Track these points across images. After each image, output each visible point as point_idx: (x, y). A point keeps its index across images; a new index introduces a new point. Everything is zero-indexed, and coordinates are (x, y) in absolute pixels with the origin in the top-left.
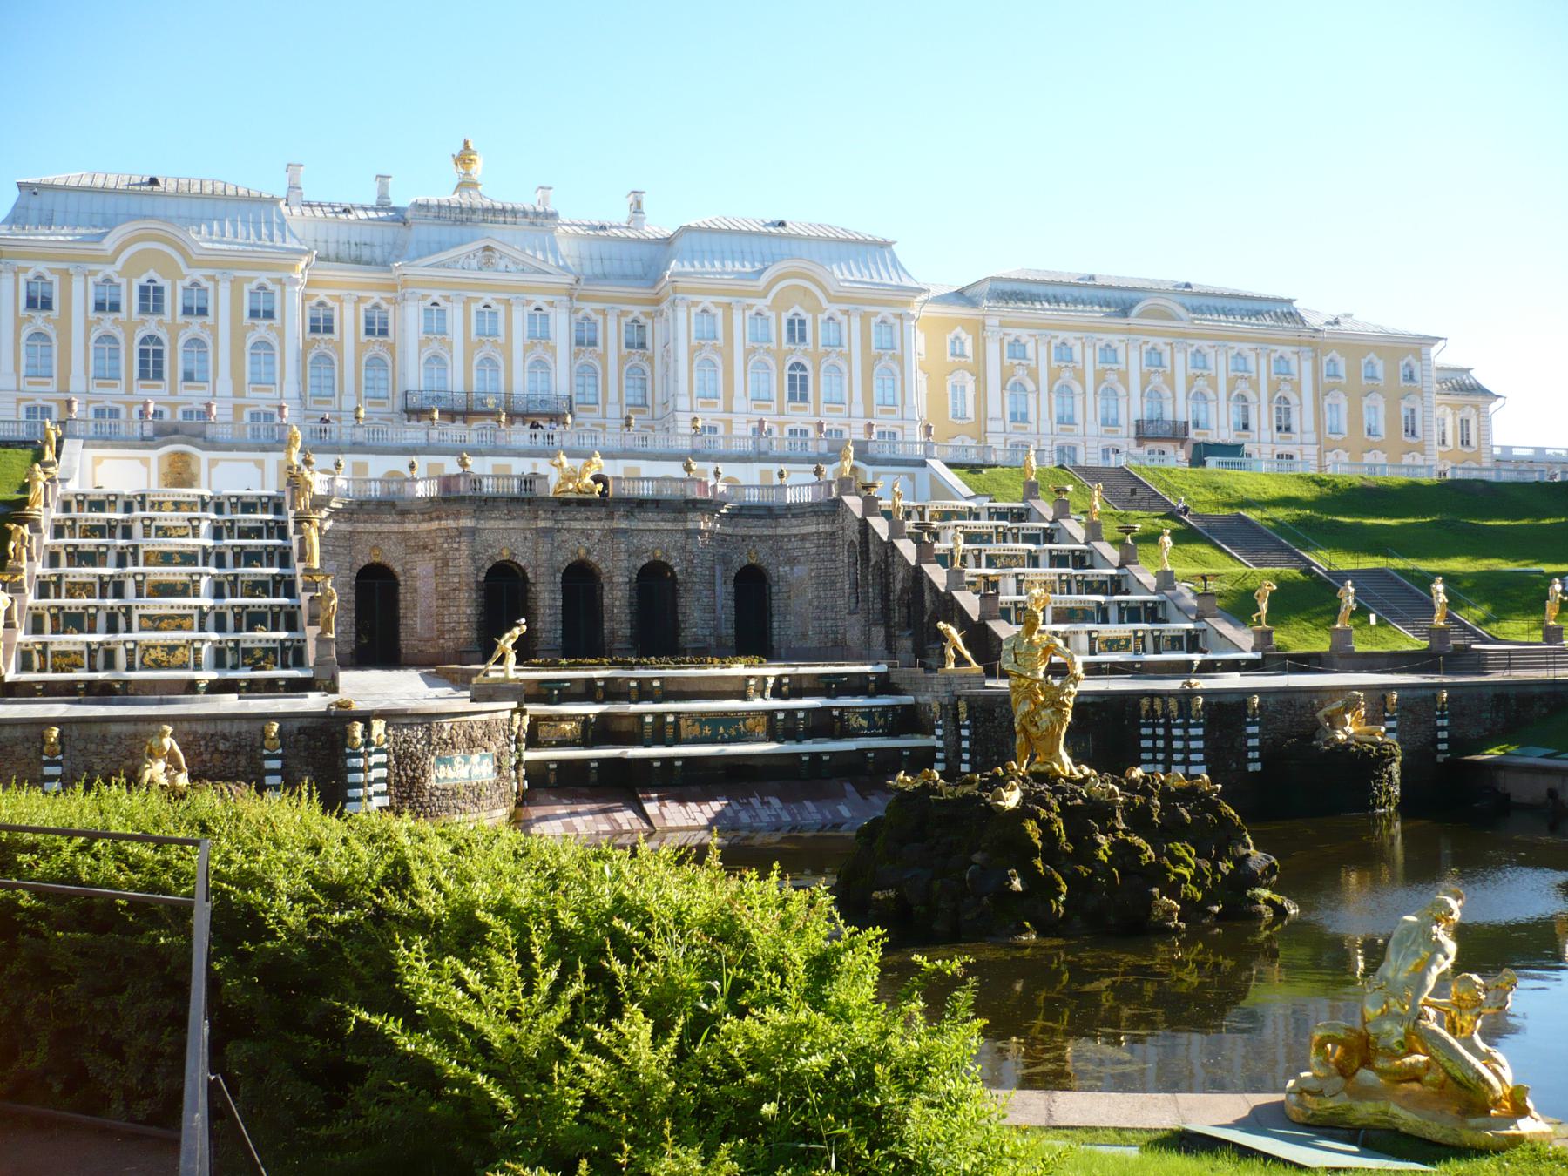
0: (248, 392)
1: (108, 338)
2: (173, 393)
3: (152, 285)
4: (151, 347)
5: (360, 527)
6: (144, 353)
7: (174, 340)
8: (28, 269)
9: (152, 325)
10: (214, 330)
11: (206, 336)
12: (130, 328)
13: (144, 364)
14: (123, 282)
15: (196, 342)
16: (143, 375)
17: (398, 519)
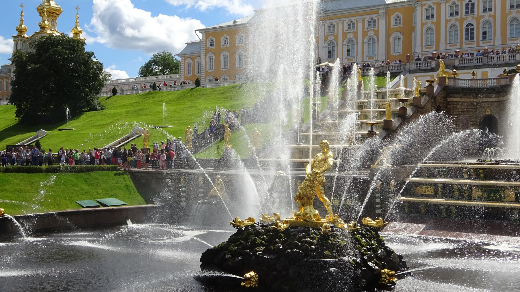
0: (508, 42)
1: (453, 26)
2: (478, 46)
3: (470, 3)
4: (470, 27)
5: (480, 100)
6: (467, 30)
7: (478, 24)
8: (425, 4)
9: (470, 19)
10: (494, 17)
11: (491, 19)
12: (461, 21)
13: (467, 34)
14: (459, 3)
15: (487, 22)
16: (467, 39)
17: (497, 95)
